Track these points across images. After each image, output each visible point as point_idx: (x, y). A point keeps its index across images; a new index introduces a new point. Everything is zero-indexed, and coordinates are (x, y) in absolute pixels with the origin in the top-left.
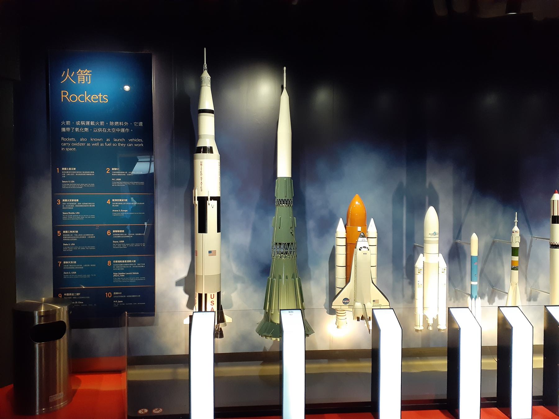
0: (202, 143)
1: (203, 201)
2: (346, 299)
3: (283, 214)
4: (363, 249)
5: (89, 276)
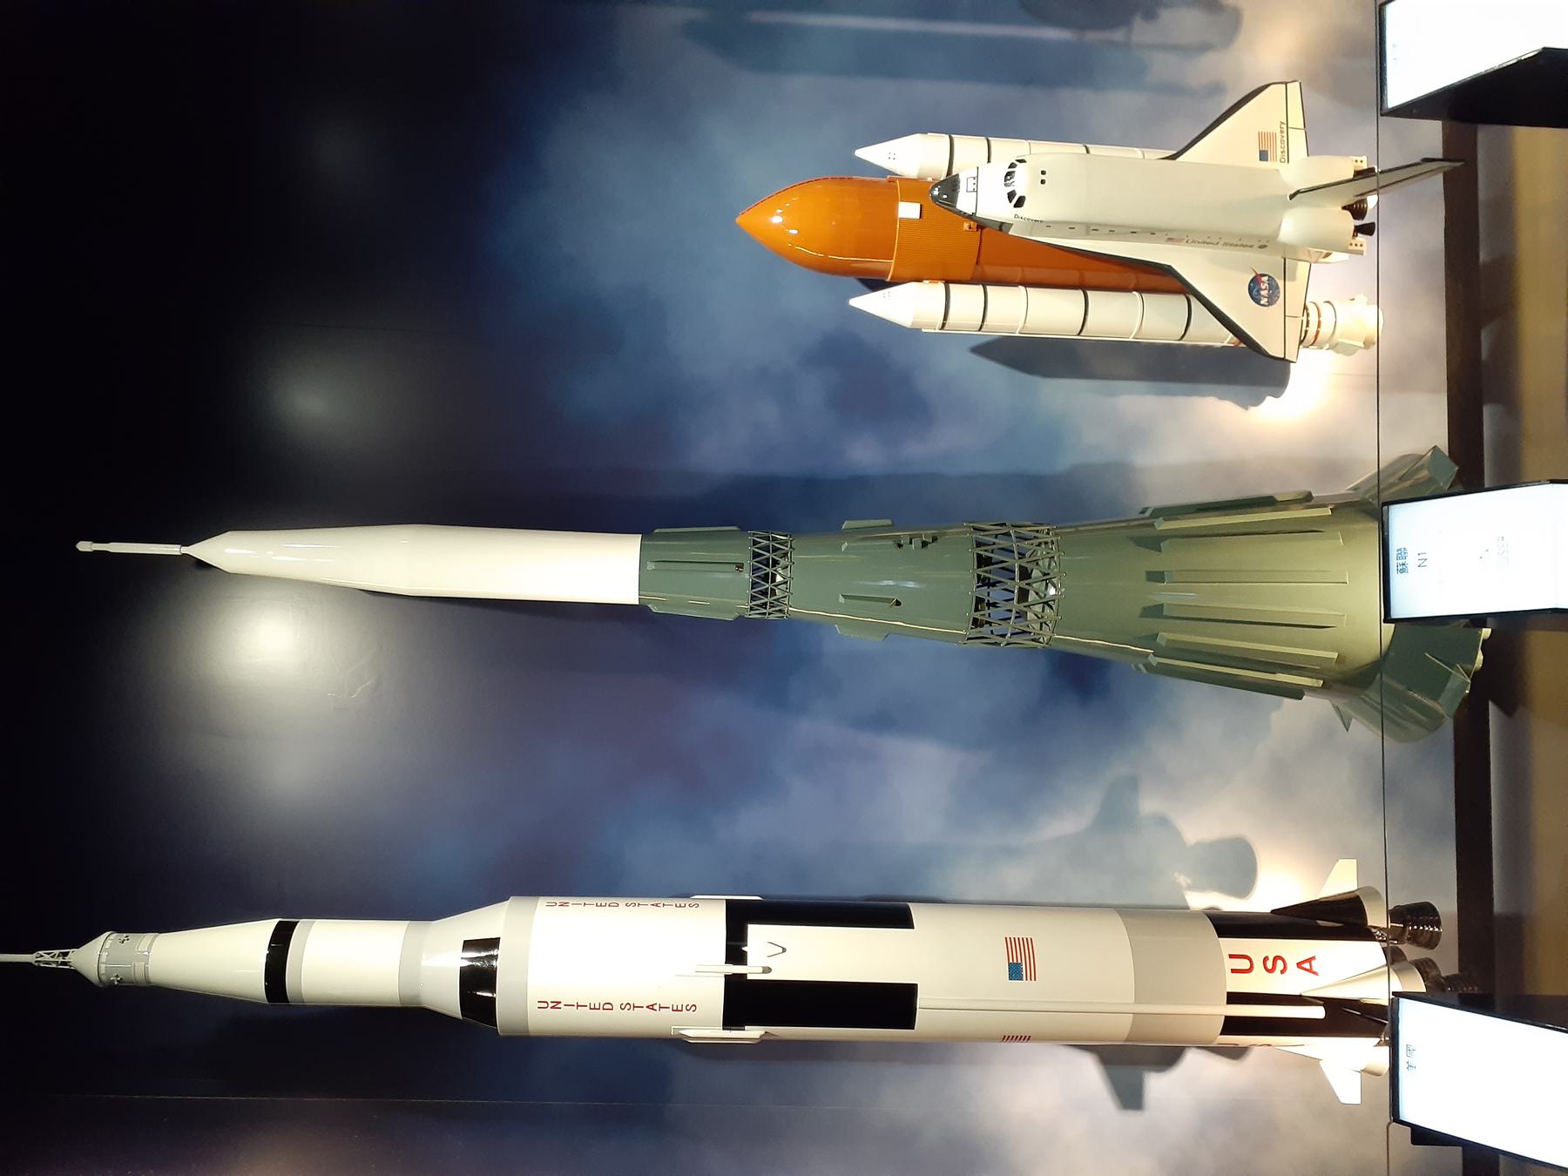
0: (446, 996)
1: (747, 1000)
2: (1254, 289)
3: (825, 585)
4: (1020, 187)
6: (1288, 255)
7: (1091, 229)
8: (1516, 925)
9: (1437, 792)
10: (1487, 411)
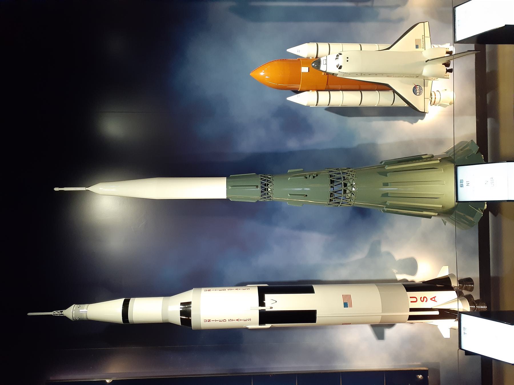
0: (176, 318)
1: (265, 317)
3: (284, 191)
6: (425, 79)
7: (362, 74)
8: (497, 280)
9: (473, 240)
10: (489, 120)
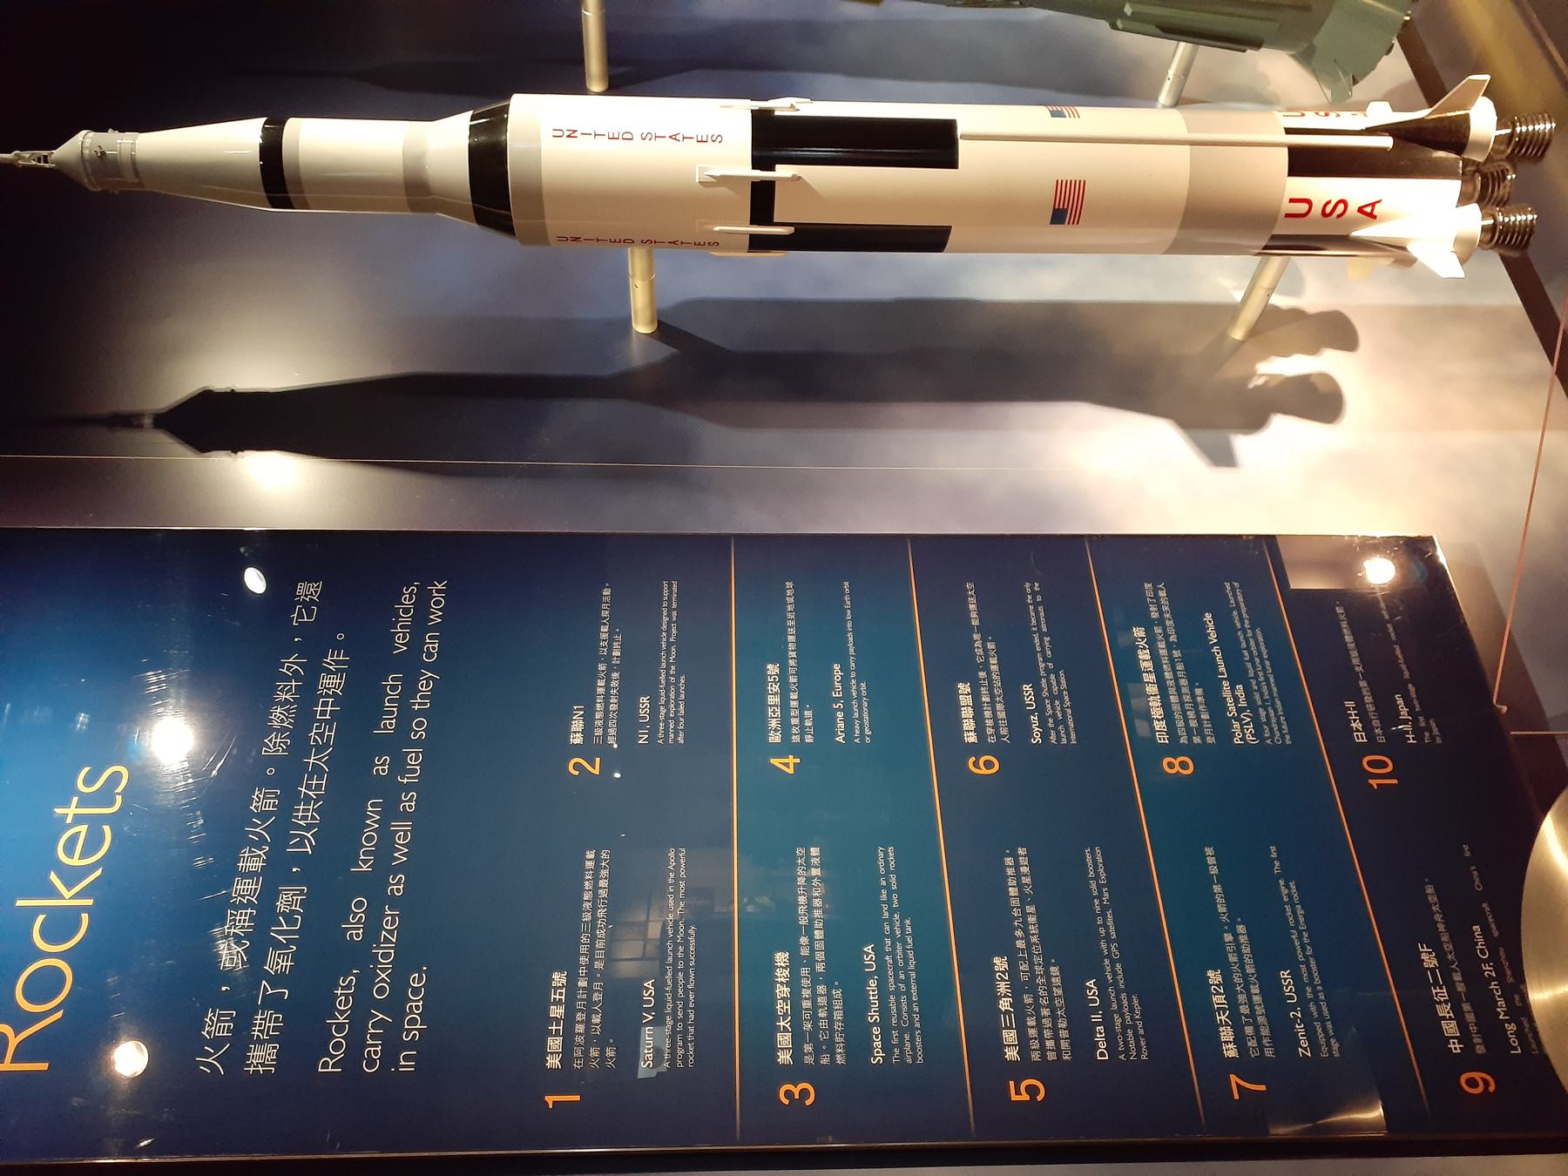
5: (1288, 890)
